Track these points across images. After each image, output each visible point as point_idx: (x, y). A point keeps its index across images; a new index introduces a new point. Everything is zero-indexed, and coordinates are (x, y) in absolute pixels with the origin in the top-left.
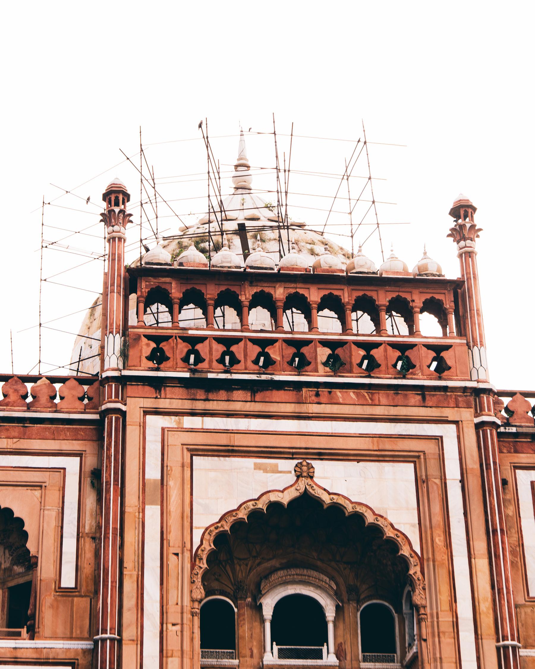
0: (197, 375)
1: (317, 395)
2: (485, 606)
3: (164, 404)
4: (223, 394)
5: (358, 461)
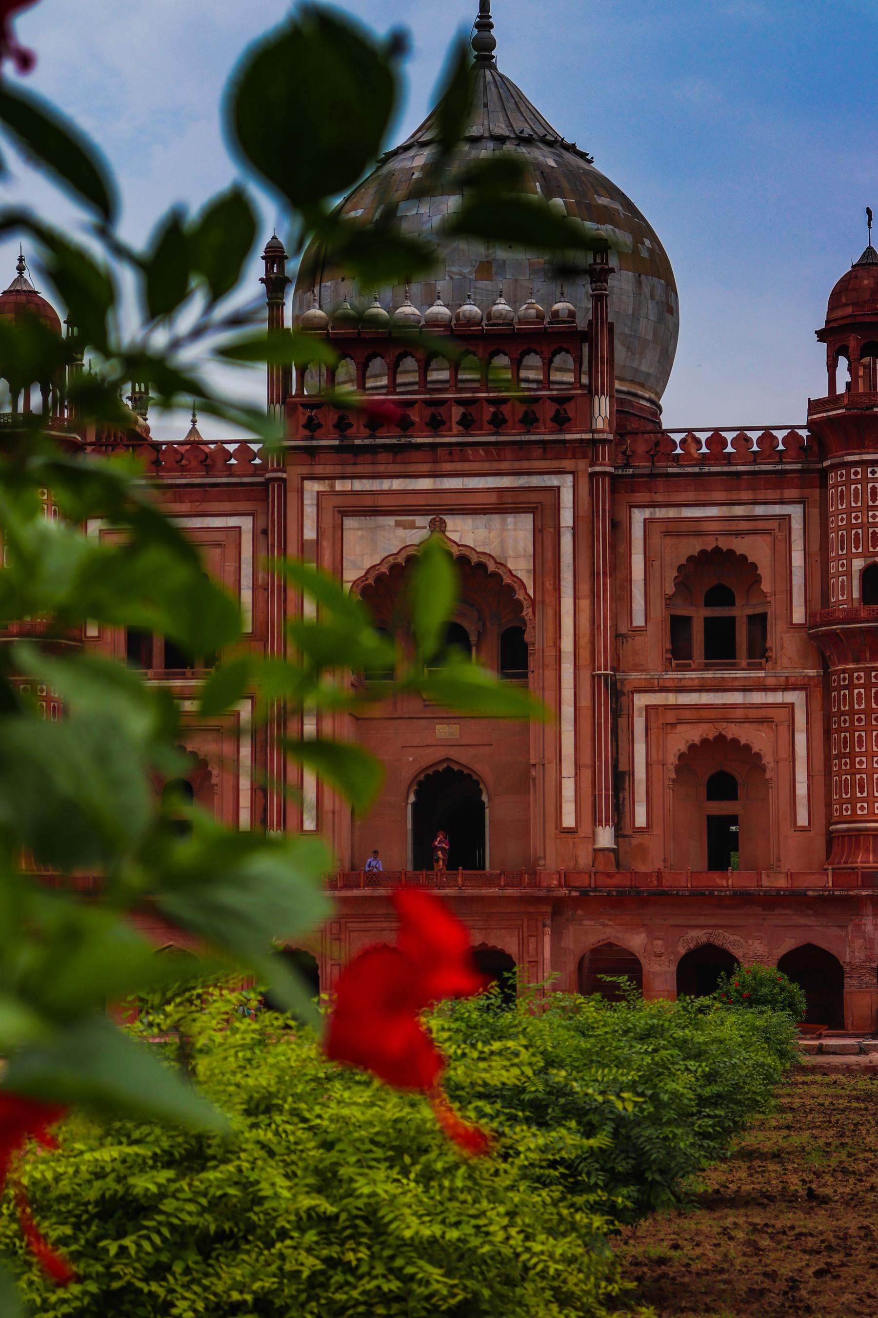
0: (346, 443)
1: (451, 454)
2: (584, 641)
3: (319, 469)
4: (369, 457)
5: (485, 514)
